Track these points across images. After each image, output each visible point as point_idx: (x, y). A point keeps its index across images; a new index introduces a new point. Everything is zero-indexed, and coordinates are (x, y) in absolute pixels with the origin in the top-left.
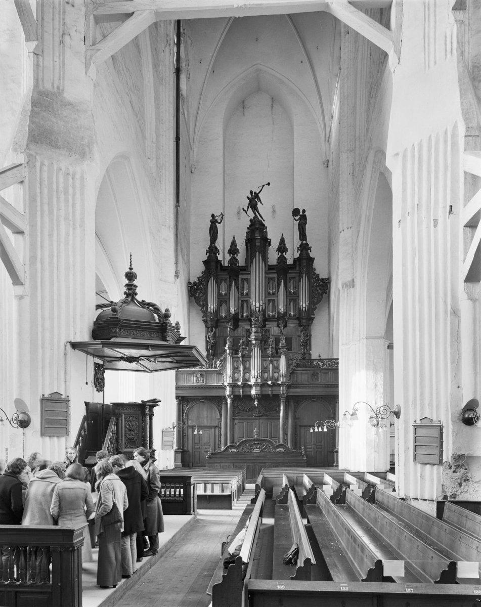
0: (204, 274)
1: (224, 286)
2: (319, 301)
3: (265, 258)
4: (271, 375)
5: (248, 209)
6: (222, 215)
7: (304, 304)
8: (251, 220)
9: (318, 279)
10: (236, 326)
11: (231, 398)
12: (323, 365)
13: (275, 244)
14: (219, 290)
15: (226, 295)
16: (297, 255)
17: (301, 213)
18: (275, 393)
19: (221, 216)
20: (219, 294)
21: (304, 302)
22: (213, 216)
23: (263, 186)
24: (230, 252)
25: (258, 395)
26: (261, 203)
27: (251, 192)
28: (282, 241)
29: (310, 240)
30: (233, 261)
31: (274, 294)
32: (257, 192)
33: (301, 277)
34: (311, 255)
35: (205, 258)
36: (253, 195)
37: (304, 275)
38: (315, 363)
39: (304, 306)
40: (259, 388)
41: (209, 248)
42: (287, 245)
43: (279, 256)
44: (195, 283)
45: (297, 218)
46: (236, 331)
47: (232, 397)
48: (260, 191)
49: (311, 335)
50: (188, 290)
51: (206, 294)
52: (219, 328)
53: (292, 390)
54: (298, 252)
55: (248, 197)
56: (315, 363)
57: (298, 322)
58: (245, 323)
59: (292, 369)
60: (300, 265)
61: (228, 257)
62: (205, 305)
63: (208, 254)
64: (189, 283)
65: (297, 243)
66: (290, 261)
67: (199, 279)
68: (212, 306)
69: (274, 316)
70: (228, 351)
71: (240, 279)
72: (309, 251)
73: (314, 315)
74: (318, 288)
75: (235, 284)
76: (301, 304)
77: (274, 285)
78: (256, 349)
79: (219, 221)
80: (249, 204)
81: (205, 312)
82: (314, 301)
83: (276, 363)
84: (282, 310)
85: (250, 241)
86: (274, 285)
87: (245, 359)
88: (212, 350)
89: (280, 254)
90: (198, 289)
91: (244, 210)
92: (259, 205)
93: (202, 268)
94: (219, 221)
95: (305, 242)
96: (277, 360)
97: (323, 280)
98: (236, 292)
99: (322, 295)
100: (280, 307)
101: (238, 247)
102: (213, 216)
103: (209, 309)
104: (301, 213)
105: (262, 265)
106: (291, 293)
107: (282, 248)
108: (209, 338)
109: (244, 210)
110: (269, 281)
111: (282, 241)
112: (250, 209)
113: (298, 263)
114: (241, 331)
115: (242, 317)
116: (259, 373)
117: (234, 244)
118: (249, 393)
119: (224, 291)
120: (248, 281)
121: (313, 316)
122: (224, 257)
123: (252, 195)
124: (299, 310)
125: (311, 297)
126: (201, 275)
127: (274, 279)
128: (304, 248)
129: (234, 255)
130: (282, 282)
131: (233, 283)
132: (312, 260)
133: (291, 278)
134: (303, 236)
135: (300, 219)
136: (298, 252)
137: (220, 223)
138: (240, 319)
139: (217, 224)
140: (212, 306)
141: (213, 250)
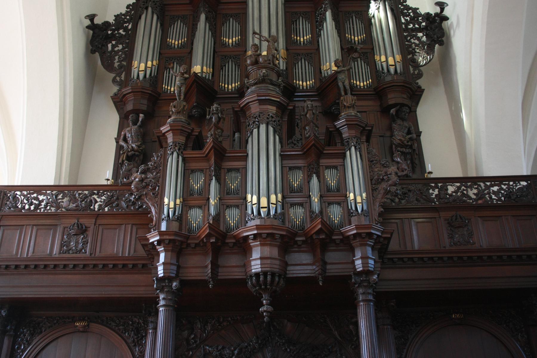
0: (131, 10)
11: (171, 292)
14: (164, 35)
18: (333, 270)
20: (164, 44)
25: (273, 274)
38: (451, 189)
39: (391, 61)
40: (275, 252)
44: (106, 24)
50: (87, 39)
59: (387, 192)
67: (117, 17)
74: (420, 35)
75: (207, 18)
78: (263, 127)
90: (112, 37)
96: (335, 167)
98: (210, 42)
108: (125, 140)
118: (237, 274)
126: (124, 10)
131: (203, 17)
138: (216, 92)
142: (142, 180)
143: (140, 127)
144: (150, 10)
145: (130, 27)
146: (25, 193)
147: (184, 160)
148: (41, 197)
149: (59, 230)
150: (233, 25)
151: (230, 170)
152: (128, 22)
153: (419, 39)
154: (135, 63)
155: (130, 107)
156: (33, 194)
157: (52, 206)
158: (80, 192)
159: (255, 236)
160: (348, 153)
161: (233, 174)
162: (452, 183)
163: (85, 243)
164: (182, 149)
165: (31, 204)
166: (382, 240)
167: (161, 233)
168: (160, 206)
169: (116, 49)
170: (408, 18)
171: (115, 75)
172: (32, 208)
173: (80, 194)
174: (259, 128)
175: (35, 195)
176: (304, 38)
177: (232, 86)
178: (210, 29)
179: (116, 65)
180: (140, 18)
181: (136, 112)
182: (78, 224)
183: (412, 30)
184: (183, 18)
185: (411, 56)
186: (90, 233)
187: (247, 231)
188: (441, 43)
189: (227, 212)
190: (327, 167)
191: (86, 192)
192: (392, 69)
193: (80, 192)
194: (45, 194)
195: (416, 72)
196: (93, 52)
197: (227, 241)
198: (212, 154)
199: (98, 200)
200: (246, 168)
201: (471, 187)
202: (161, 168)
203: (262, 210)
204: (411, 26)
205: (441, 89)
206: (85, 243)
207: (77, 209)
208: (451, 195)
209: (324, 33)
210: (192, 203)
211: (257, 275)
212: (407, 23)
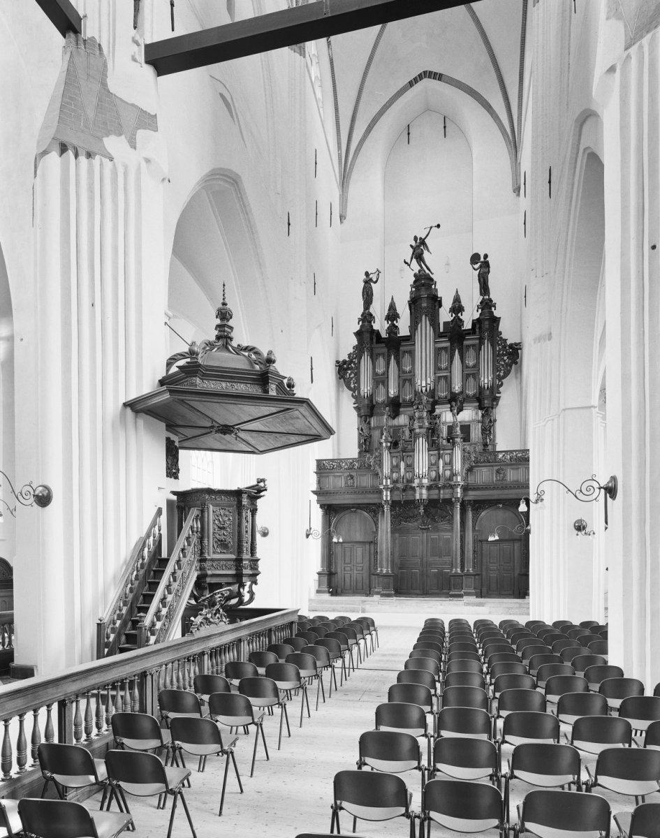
2: (507, 374)
5: (411, 261)
7: (486, 379)
8: (415, 275)
10: (395, 414)
13: (447, 303)
14: (374, 368)
15: (383, 374)
16: (477, 315)
17: (482, 259)
20: (375, 374)
21: (486, 377)
22: (367, 274)
23: (431, 227)
24: (388, 318)
26: (428, 251)
27: (416, 238)
28: (457, 300)
29: (494, 295)
30: (393, 329)
31: (446, 369)
33: (481, 343)
34: (496, 313)
35: (357, 328)
36: (418, 241)
37: (486, 341)
38: (500, 456)
39: (486, 381)
41: (362, 315)
44: (344, 362)
45: (476, 266)
46: (396, 420)
47: (390, 502)
48: (426, 238)
49: (495, 421)
51: (357, 375)
53: (471, 493)
54: (478, 311)
55: (411, 246)
60: (480, 328)
61: (387, 326)
62: (357, 388)
63: (361, 323)
64: (338, 362)
65: (478, 299)
66: (468, 325)
67: (349, 355)
68: (366, 388)
69: (446, 397)
70: (384, 444)
72: (493, 309)
73: (500, 393)
74: (505, 358)
76: (482, 379)
77: (444, 357)
79: (374, 280)
80: (413, 254)
81: (357, 398)
82: (499, 375)
83: (447, 458)
84: (457, 388)
85: (414, 303)
88: (365, 444)
89: (454, 315)
90: (348, 369)
91: (406, 263)
92: (426, 255)
93: (354, 341)
94: (374, 280)
95: (487, 297)
97: (511, 346)
98: (397, 372)
100: (453, 386)
101: (399, 311)
103: (362, 393)
104: (482, 259)
107: (457, 308)
108: (362, 430)
109: (406, 263)
110: (438, 351)
111: (457, 300)
112: (414, 260)
113: (478, 326)
114: (402, 420)
115: (404, 400)
117: (392, 307)
118: (411, 498)
120: (412, 353)
121: (498, 395)
122: (380, 325)
123: (416, 241)
124: (481, 389)
125: (496, 369)
126: (352, 351)
127: (445, 348)
128: (487, 305)
129: (392, 321)
131: (393, 357)
132: (496, 321)
133: (468, 346)
134: (484, 289)
135: (481, 267)
136: (478, 311)
137: (375, 282)
140: (366, 388)
141: (367, 318)
152: (355, 358)
154: (362, 388)
164: (389, 448)
168: (382, 471)
179: (352, 386)
184: (383, 354)
188: (516, 363)
200: (414, 455)
202: (381, 455)
211: (418, 500)
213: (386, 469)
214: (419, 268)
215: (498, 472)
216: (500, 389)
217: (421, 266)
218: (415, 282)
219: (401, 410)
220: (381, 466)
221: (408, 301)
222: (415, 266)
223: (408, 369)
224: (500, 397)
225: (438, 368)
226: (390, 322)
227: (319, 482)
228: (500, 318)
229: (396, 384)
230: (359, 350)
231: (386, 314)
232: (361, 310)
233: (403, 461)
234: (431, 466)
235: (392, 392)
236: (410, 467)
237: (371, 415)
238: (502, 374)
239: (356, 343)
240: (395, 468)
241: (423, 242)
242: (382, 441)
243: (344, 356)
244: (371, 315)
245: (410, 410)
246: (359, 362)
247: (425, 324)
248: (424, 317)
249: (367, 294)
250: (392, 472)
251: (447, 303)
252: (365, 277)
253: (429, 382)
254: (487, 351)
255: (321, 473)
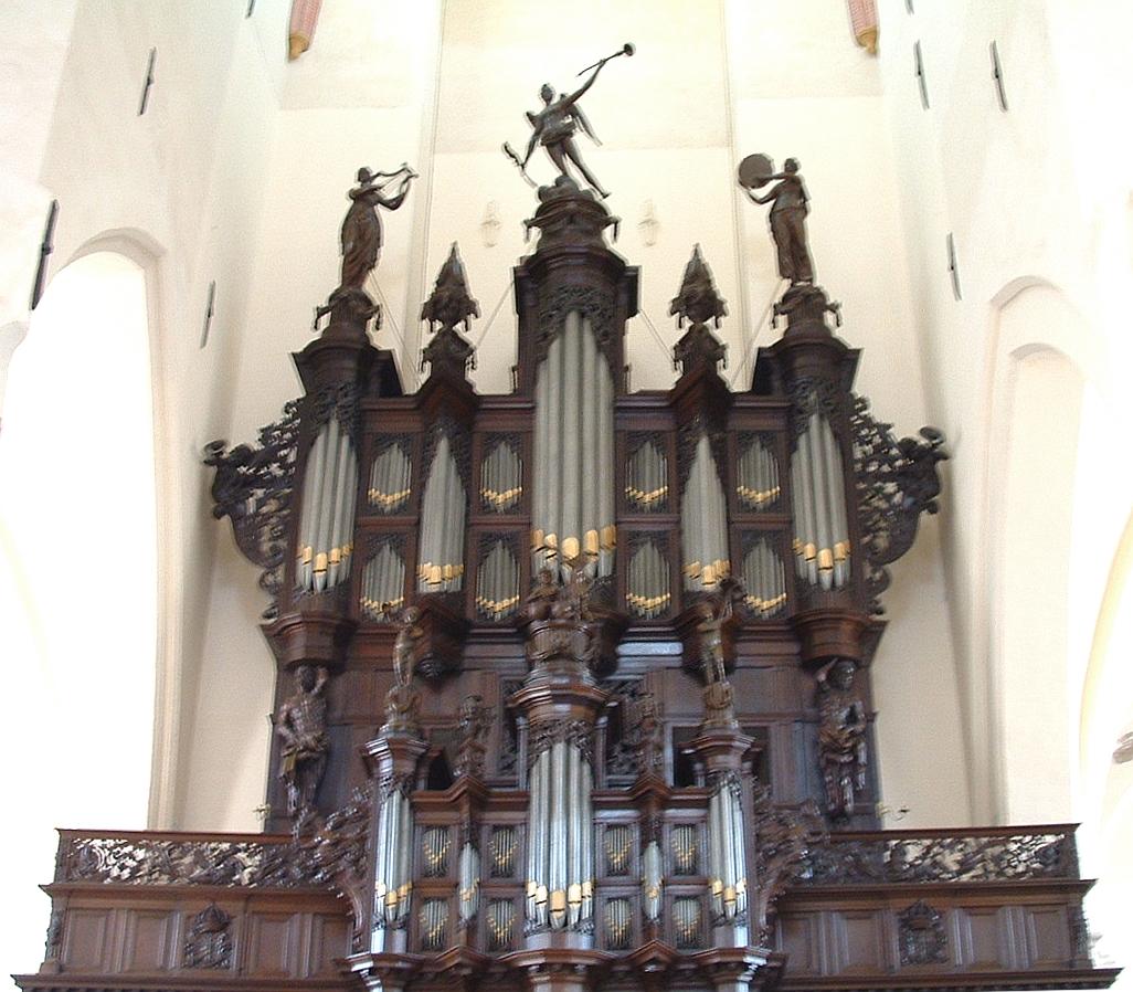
1: (393, 470)
3: (611, 346)
4: (653, 911)
6: (407, 175)
8: (542, 193)
9: (882, 451)
10: (442, 670)
12: (965, 866)
13: (659, 288)
16: (770, 336)
19: (403, 176)
20: (363, 505)
22: (364, 175)
24: (432, 310)
27: (546, 94)
29: (827, 276)
30: (450, 356)
32: (570, 92)
34: (847, 334)
37: (814, 420)
38: (913, 852)
39: (825, 558)
42: (724, 286)
43: (684, 332)
44: (243, 454)
45: (762, 192)
49: (871, 717)
50: (204, 483)
51: (293, 505)
52: (354, 674)
56: (913, 852)
57: (794, 648)
58: (499, 649)
60: (788, 376)
61: (426, 335)
62: (289, 557)
63: (325, 321)
66: (736, 375)
67: (266, 433)
69: (664, 612)
70: (386, 767)
71: (477, 439)
72: (829, 318)
73: (880, 612)
74: (890, 487)
75: (452, 450)
76: (809, 550)
77: (652, 463)
80: (537, 134)
81: (284, 593)
82: (871, 546)
84: (707, 571)
85: (530, 279)
86: (652, 463)
87: (493, 817)
88: (299, 784)
89: (688, 324)
92: (579, 139)
94: (390, 193)
97: (908, 447)
99: (911, 515)
101: (475, 290)
102: (364, 175)
103: (304, 573)
105: (596, 370)
106: (748, 507)
107: (698, 299)
108: (289, 722)
110: (626, 447)
112: (541, 152)
115: (483, 613)
116: (575, 893)
117: (451, 277)
119: (389, 495)
120: (523, 443)
124: (799, 587)
125: (858, 525)
126: (278, 418)
130: (703, 447)
131: (443, 446)
132: (845, 360)
134: (793, 253)
135: (774, 194)
137: (395, 204)
138: (470, 625)
139: (380, 210)
142: (335, 844)
143: (319, 695)
144: (334, 425)
145: (292, 459)
146: (110, 843)
147: (413, 806)
148: (140, 854)
149: (178, 919)
150: (504, 457)
151: (496, 828)
153: (889, 497)
154: (306, 552)
155: (297, 653)
156: (126, 845)
157: (161, 872)
158: (213, 845)
159: (542, 968)
160: (715, 799)
161: (503, 836)
162: (919, 839)
163: (228, 948)
164: (407, 785)
165: (122, 868)
166: (766, 971)
167: (374, 957)
169: (265, 509)
170: (869, 448)
171: (263, 571)
172: (126, 873)
173: (214, 850)
174: (551, 749)
175: (130, 848)
176: (651, 495)
177: (501, 605)
178: (459, 473)
179: (266, 547)
180: (312, 444)
181: (311, 664)
182: (214, 911)
183: (879, 476)
185: (866, 539)
186: (236, 928)
187: (529, 958)
188: (933, 509)
189: (492, 910)
190: (677, 826)
191: (225, 846)
192: (826, 576)
193: (213, 845)
194: (148, 848)
195: (878, 575)
196: (218, 515)
197: (492, 970)
198: (464, 799)
199: (249, 862)
200: (526, 823)
201: (951, 847)
203: (555, 915)
204: (872, 468)
205: (937, 589)
206: (228, 948)
207: (208, 880)
208: (912, 865)
209: (692, 484)
210: (429, 892)
212: (866, 461)
213: (387, 887)
214: (559, 173)
215: (910, 924)
216: (883, 598)
217: (561, 166)
218: (540, 212)
219: (472, 650)
220: (364, 872)
221: (515, 270)
222: (544, 170)
223: (502, 497)
224: (883, 624)
225: (623, 506)
226: (438, 325)
227: (56, 937)
228: (857, 352)
229: (455, 547)
230: (305, 420)
231: (427, 299)
232: (334, 282)
233: (476, 847)
234: (610, 877)
235: (435, 574)
236: (504, 882)
237: (335, 669)
238: (882, 542)
239: (297, 391)
240: (429, 884)
241: (569, 106)
242: (377, 747)
243: (245, 434)
244: (367, 301)
245: (509, 656)
246: (303, 460)
247: (574, 343)
248: (572, 320)
249: (361, 237)
250: (419, 896)
251: (659, 288)
252: (357, 186)
253: (591, 546)
254: (816, 452)
255: (70, 893)
